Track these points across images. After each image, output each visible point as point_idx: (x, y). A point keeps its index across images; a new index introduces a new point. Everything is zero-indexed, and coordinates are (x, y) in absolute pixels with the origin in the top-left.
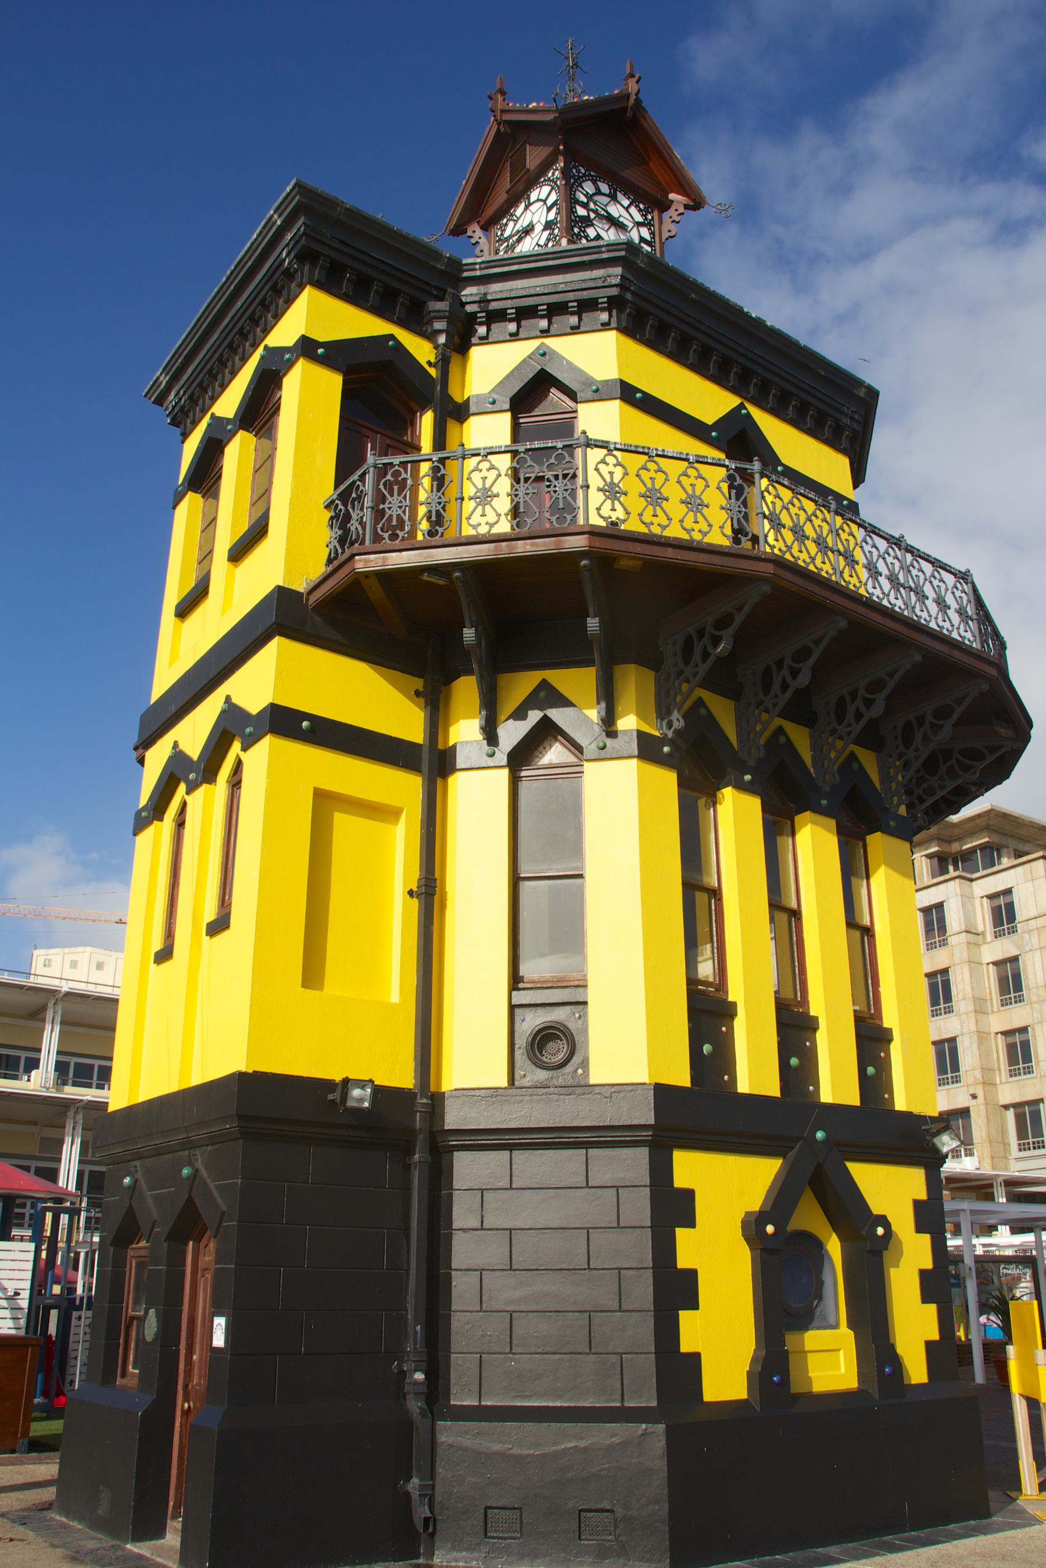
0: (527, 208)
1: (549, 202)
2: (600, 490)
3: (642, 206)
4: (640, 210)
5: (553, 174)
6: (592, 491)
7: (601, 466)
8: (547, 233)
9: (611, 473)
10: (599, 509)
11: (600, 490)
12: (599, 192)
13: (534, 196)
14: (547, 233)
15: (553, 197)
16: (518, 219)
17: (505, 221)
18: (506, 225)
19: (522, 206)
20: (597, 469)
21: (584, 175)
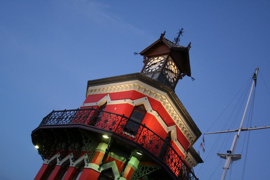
0: (157, 59)
1: (162, 62)
2: (142, 136)
3: (178, 70)
4: (178, 71)
5: (165, 57)
6: (141, 136)
7: (145, 132)
8: (158, 68)
9: (146, 134)
10: (140, 140)
11: (142, 136)
12: (172, 65)
13: (160, 58)
14: (158, 68)
15: (163, 61)
16: (155, 60)
17: (152, 58)
18: (152, 59)
19: (156, 58)
20: (144, 132)
21: (171, 60)
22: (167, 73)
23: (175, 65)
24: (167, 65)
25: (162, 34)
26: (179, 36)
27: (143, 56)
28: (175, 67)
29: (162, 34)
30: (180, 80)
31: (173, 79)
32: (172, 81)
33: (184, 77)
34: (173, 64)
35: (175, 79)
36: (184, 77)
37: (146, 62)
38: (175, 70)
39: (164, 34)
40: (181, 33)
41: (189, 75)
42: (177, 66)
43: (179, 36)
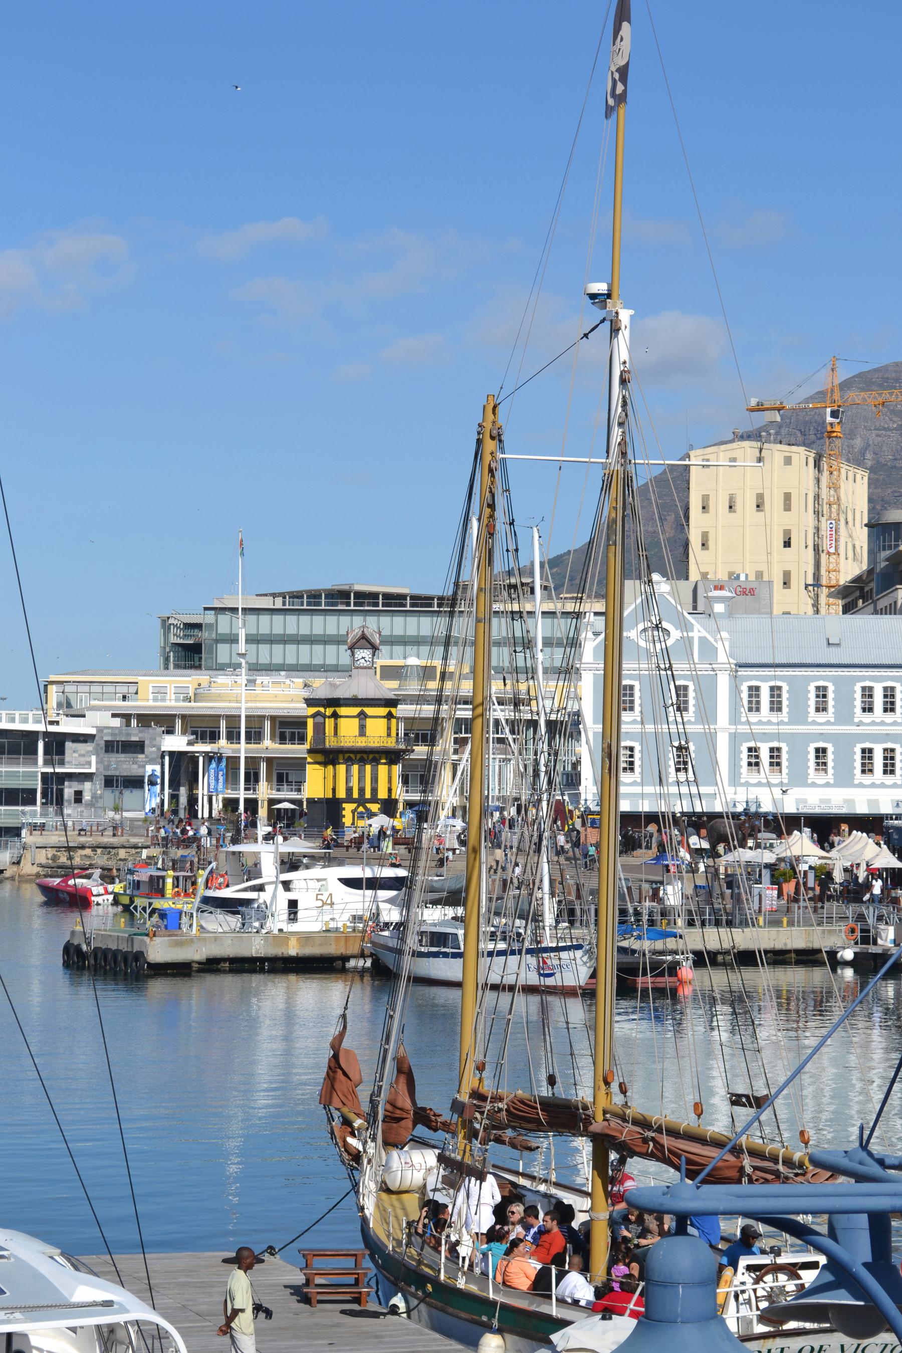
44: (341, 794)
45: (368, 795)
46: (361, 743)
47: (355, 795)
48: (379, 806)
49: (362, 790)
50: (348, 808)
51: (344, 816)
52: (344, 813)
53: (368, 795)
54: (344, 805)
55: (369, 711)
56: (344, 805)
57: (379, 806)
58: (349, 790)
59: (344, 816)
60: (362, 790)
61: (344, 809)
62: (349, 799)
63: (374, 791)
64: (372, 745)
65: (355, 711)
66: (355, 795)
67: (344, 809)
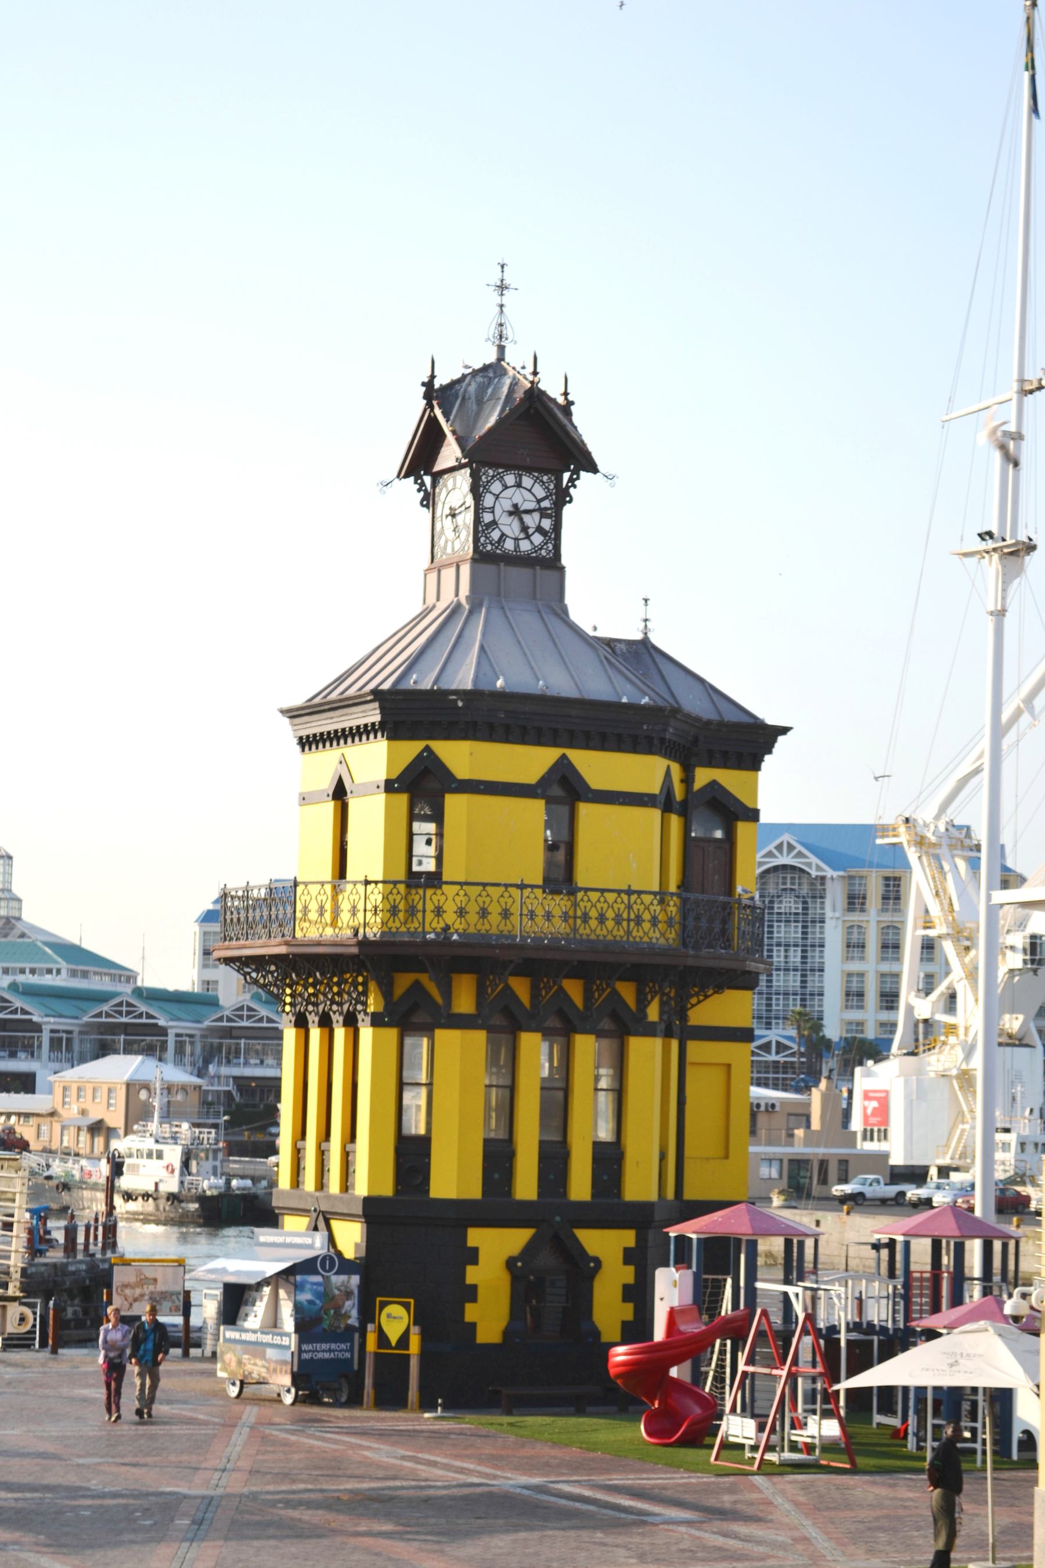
3: (545, 478)
12: (506, 487)
21: (493, 477)
22: (503, 535)
23: (520, 476)
24: (484, 509)
25: (423, 384)
26: (502, 306)
27: (412, 479)
28: (527, 481)
29: (423, 384)
30: (567, 510)
31: (539, 529)
32: (537, 539)
33: (575, 487)
34: (510, 479)
35: (547, 524)
36: (575, 487)
37: (428, 500)
38: (530, 491)
39: (433, 377)
40: (502, 287)
41: (593, 468)
42: (529, 470)
43: (502, 306)
44: (453, 1177)
45: (580, 1186)
46: (543, 919)
47: (526, 1185)
48: (628, 1238)
49: (554, 1160)
50: (495, 1247)
51: (471, 1293)
52: (473, 1275)
53: (580, 1186)
54: (475, 1237)
55: (598, 767)
56: (475, 1237)
57: (628, 1238)
58: (498, 1158)
59: (471, 1293)
60: (554, 1160)
61: (473, 1256)
62: (495, 1206)
63: (609, 1159)
64: (591, 930)
65: (532, 762)
66: (526, 1185)
67: (473, 1256)
